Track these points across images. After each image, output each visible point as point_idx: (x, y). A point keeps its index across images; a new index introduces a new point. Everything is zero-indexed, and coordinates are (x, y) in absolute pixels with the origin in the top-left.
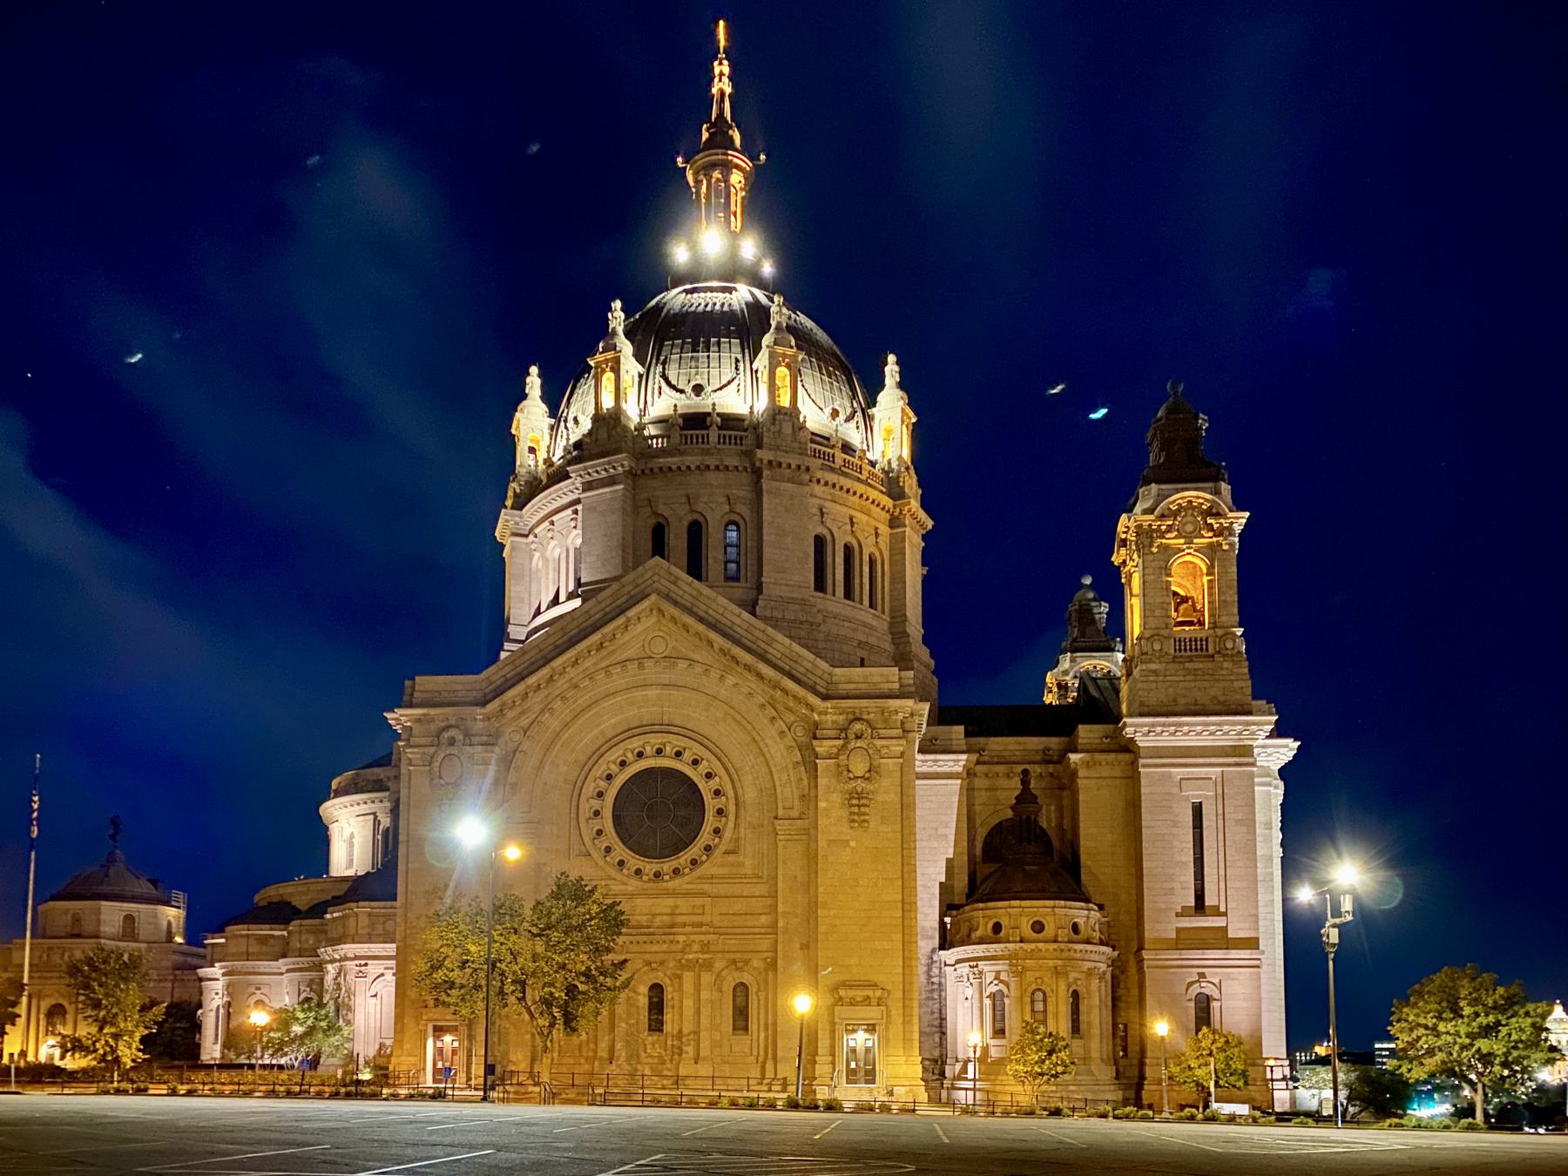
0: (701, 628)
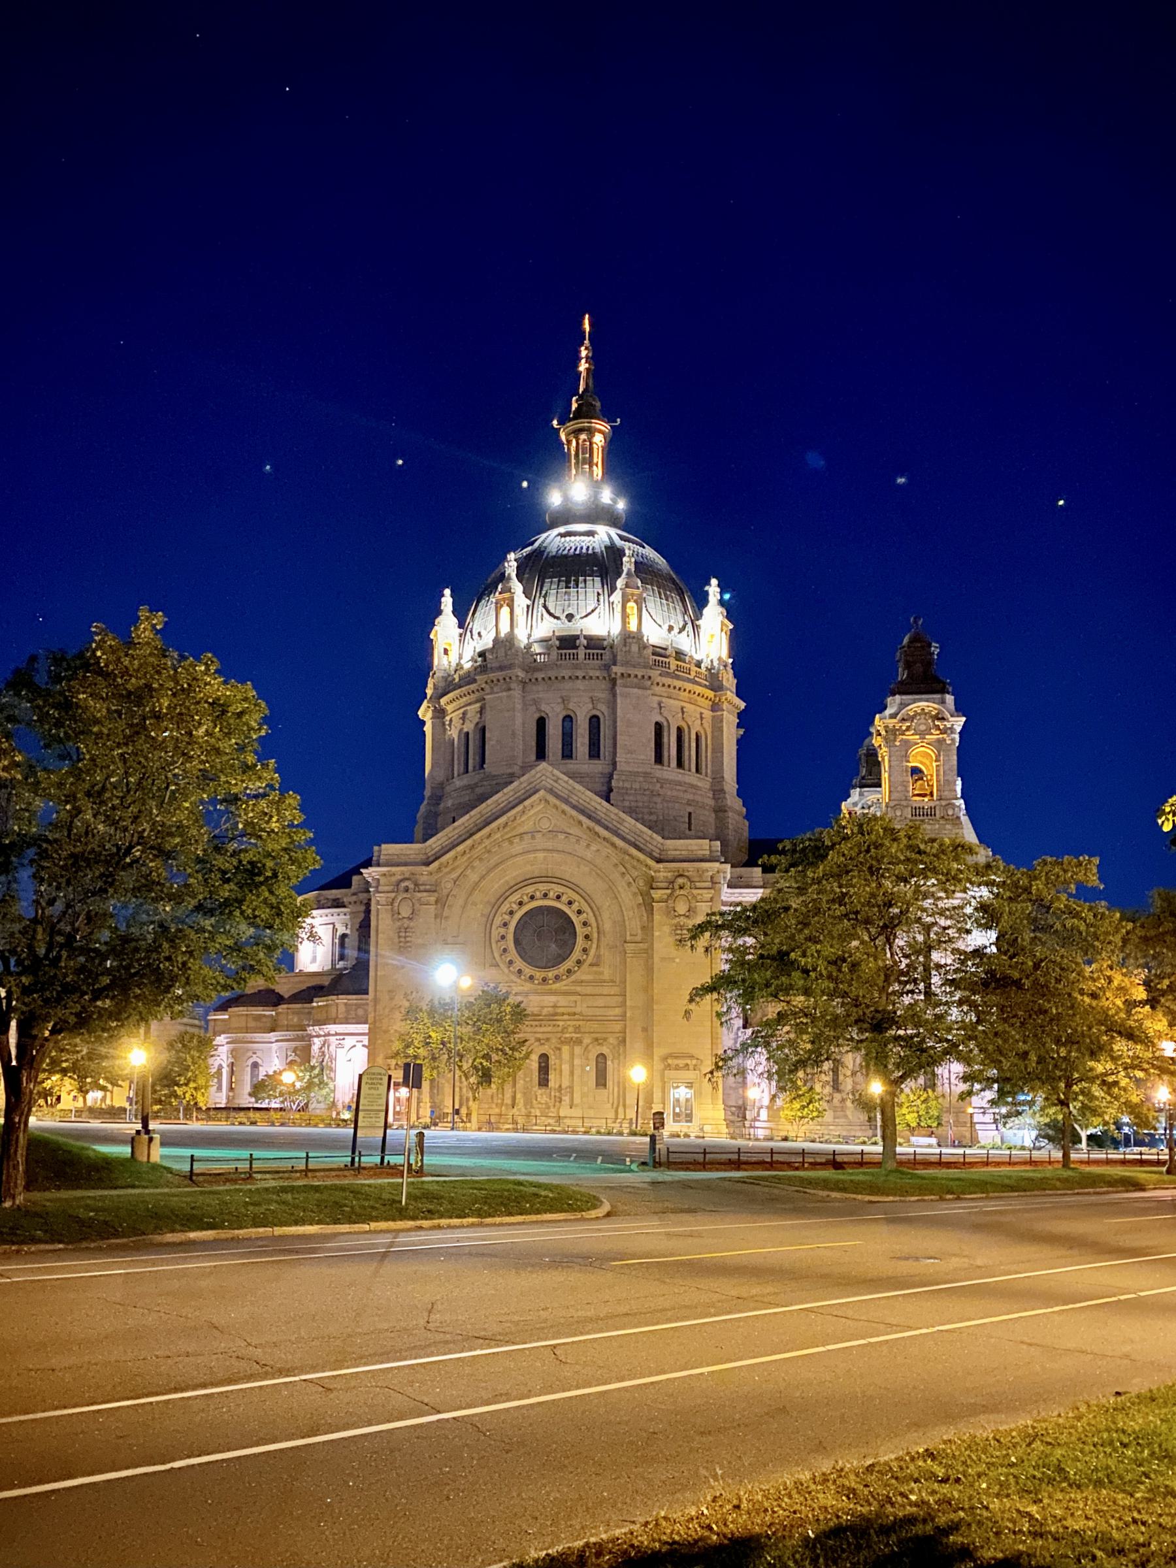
0: (574, 813)
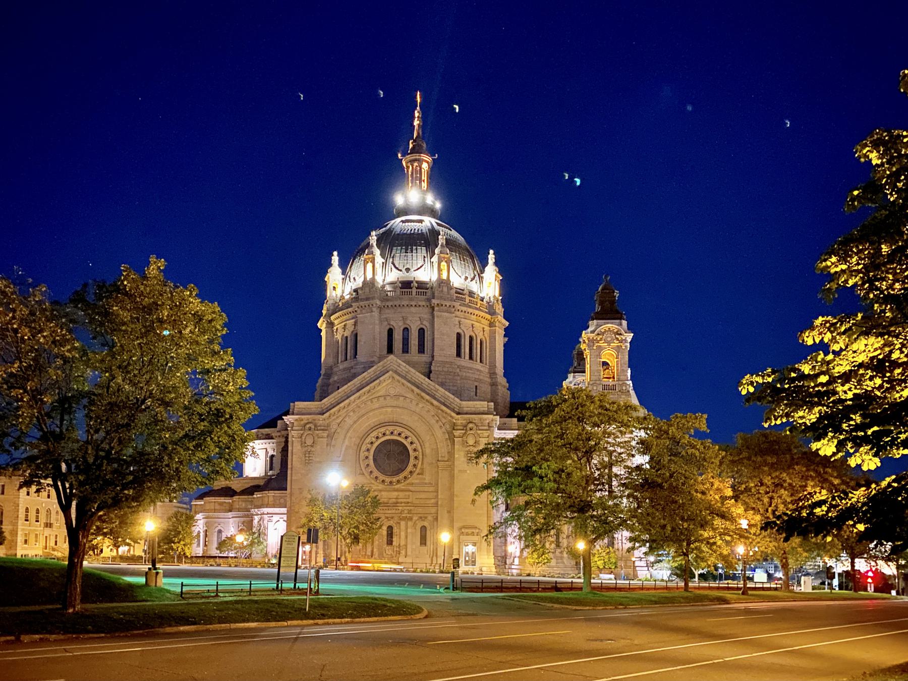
0: (409, 385)
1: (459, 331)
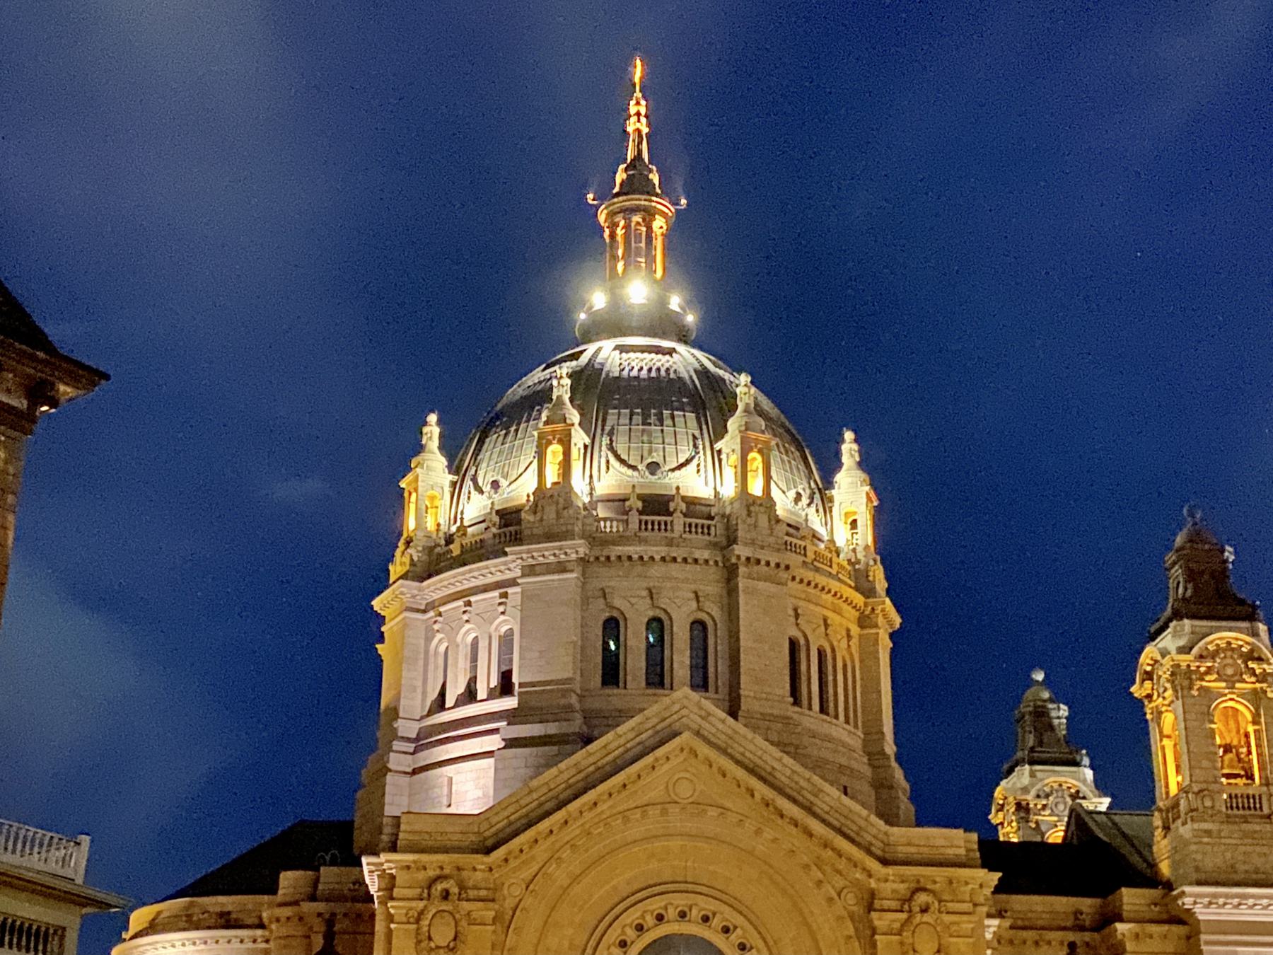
0: (740, 773)
1: (794, 632)
